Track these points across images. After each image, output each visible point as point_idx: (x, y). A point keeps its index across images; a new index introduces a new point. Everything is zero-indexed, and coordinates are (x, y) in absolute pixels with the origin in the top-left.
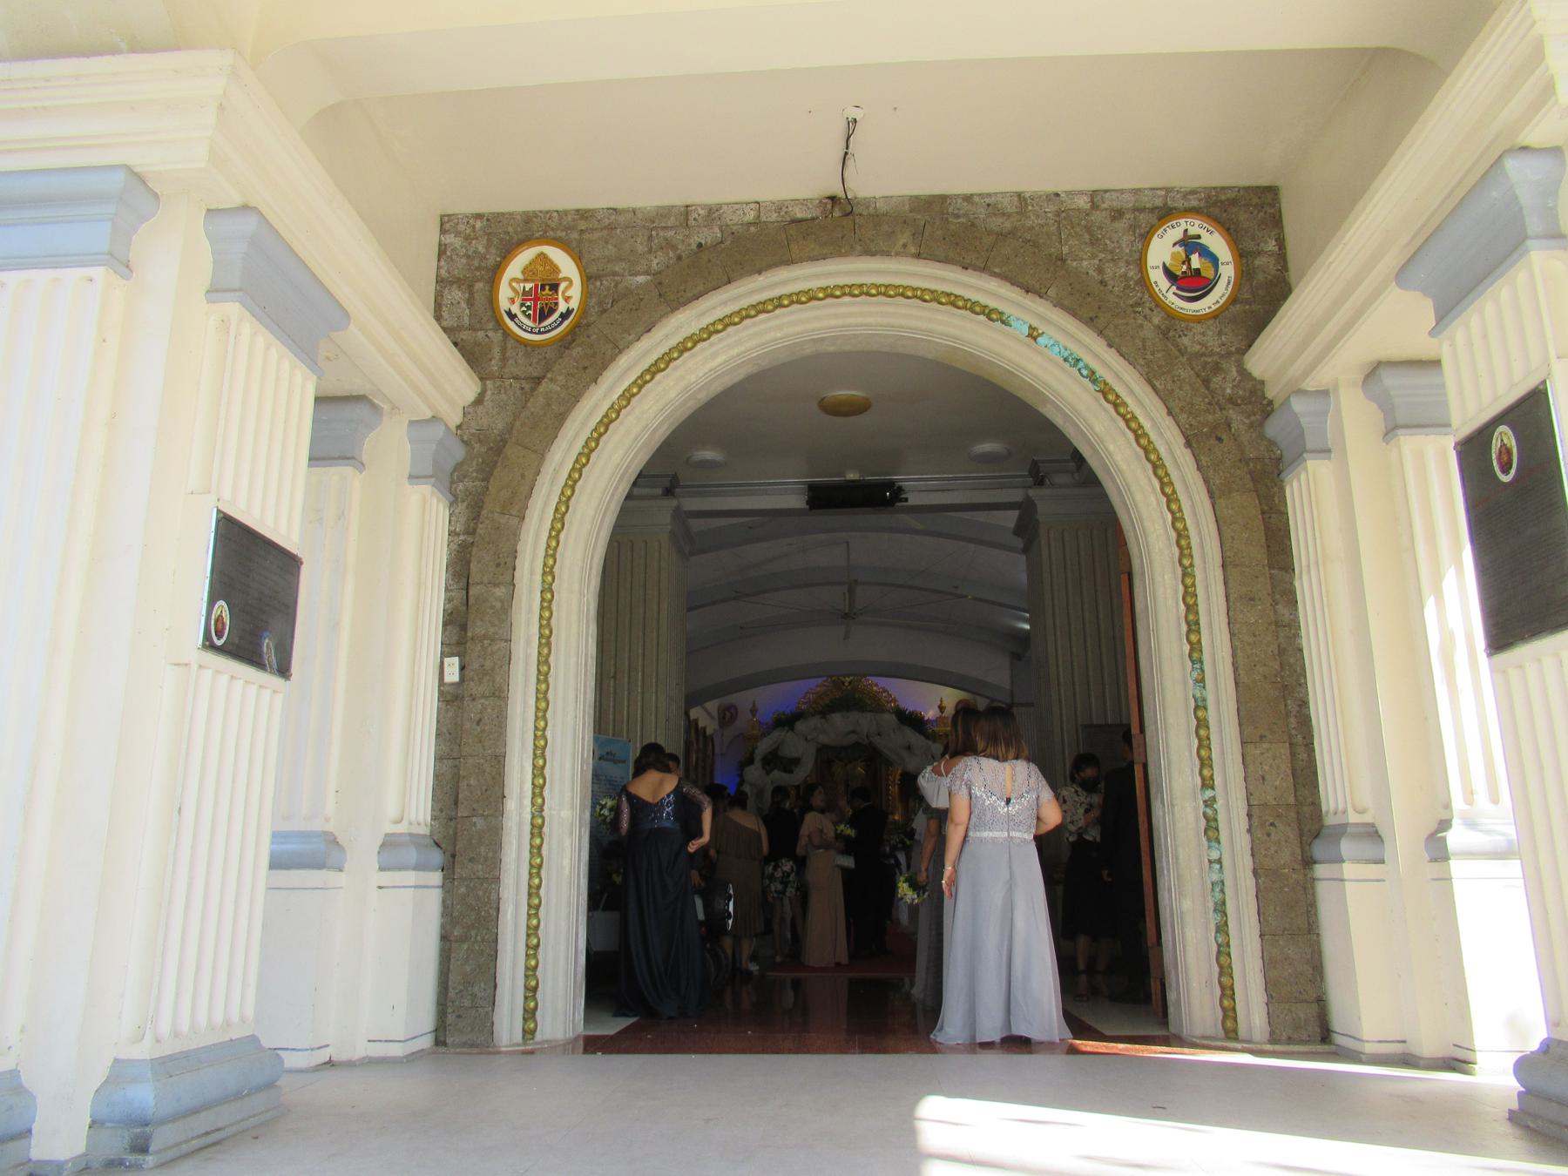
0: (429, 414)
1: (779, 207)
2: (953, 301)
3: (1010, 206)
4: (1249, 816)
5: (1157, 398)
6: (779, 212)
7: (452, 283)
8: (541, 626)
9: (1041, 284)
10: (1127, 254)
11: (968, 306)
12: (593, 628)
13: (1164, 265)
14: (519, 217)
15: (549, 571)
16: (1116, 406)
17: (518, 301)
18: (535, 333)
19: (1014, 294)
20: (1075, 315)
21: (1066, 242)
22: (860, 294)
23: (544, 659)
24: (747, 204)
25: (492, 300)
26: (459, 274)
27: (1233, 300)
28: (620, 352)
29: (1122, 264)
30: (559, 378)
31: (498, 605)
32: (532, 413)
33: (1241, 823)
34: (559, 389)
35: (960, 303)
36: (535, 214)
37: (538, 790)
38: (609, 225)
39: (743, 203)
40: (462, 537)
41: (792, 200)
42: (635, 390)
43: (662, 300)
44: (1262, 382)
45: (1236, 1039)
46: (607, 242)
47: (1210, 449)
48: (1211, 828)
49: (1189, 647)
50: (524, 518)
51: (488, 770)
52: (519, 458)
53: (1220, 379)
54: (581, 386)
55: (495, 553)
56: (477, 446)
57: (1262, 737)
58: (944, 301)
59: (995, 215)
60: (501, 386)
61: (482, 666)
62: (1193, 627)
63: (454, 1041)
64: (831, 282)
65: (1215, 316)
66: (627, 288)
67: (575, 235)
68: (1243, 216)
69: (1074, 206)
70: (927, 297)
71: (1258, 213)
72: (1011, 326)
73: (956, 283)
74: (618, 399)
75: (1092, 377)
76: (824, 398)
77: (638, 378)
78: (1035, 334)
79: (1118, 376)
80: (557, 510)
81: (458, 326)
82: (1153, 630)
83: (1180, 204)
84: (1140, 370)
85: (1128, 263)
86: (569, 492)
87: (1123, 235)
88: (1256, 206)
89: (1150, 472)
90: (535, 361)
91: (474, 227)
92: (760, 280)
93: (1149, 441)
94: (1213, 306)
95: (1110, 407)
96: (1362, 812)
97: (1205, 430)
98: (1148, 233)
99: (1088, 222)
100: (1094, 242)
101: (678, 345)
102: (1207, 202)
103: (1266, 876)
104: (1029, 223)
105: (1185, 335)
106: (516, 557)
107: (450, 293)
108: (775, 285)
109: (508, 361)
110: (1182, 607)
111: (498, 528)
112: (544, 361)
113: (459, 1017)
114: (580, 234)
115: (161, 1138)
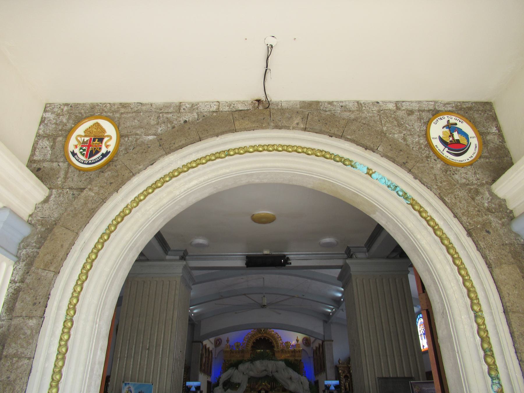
2: (324, 155)
5: (446, 207)
6: (230, 107)
7: (44, 137)
8: (60, 345)
9: (374, 145)
10: (418, 132)
11: (332, 157)
12: (104, 343)
13: (440, 137)
14: (88, 105)
15: (72, 308)
16: (420, 212)
17: (79, 147)
18: (86, 164)
19: (359, 150)
20: (394, 161)
21: (385, 125)
22: (273, 150)
23: (57, 370)
25: (65, 146)
26: (49, 132)
27: (480, 156)
28: (134, 175)
30: (95, 188)
31: (29, 332)
32: (75, 208)
35: (328, 156)
40: (18, 285)
42: (142, 198)
44: (504, 200)
46: (134, 119)
47: (484, 238)
49: (487, 366)
50: (59, 273)
52: (61, 234)
53: (480, 197)
54: (107, 193)
55: (34, 296)
56: (39, 227)
58: (319, 154)
59: (345, 111)
60: (61, 193)
61: (8, 378)
64: (257, 143)
65: (471, 164)
66: (142, 142)
68: (476, 116)
69: (387, 108)
70: (310, 152)
71: (484, 114)
72: (356, 168)
73: (327, 144)
74: (131, 202)
75: (405, 196)
76: (253, 215)
77: (144, 191)
78: (371, 172)
80: (84, 267)
81: (43, 159)
82: (458, 352)
83: (442, 108)
84: (435, 191)
85: (419, 136)
86: (93, 257)
88: (482, 111)
89: (445, 251)
91: (63, 110)
93: (442, 233)
94: (469, 159)
95: (417, 213)
97: (478, 226)
98: (428, 122)
99: (395, 116)
100: (400, 125)
101: (169, 173)
102: (456, 108)
104: (364, 115)
105: (456, 174)
106: (49, 298)
109: (68, 179)
110: (478, 338)
111: (39, 279)
112: (90, 179)
114: (121, 115)
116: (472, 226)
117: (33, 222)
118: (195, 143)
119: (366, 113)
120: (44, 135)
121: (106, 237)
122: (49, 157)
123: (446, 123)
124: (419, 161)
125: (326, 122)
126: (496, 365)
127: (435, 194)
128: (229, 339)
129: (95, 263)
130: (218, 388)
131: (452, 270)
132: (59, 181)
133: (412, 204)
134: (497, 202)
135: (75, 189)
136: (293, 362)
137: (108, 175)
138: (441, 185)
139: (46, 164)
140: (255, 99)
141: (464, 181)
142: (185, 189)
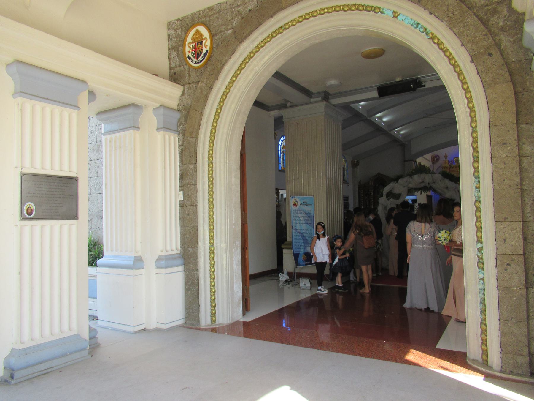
0: (158, 105)
7: (172, 49)
14: (190, 16)
28: (224, 65)
30: (204, 81)
31: (191, 172)
32: (197, 96)
33: (493, 262)
36: (195, 14)
37: (211, 238)
42: (234, 79)
43: (236, 39)
46: (218, 19)
48: (480, 262)
49: (474, 170)
50: (198, 138)
55: (189, 153)
57: (505, 219)
60: (189, 87)
61: (188, 194)
77: (234, 73)
79: (436, 29)
89: (457, 77)
90: (198, 74)
92: (273, 20)
103: (502, 290)
106: (197, 153)
107: (172, 53)
108: (279, 21)
109: (191, 76)
113: (189, 315)
114: (210, 18)
115: (17, 375)
116: (475, 52)
117: (180, 109)
118: (258, 28)
120: (172, 48)
121: (219, 111)
122: (178, 64)
128: (447, 155)
129: (217, 128)
130: (382, 198)
138: (452, 15)
139: (178, 69)
142: (262, 64)
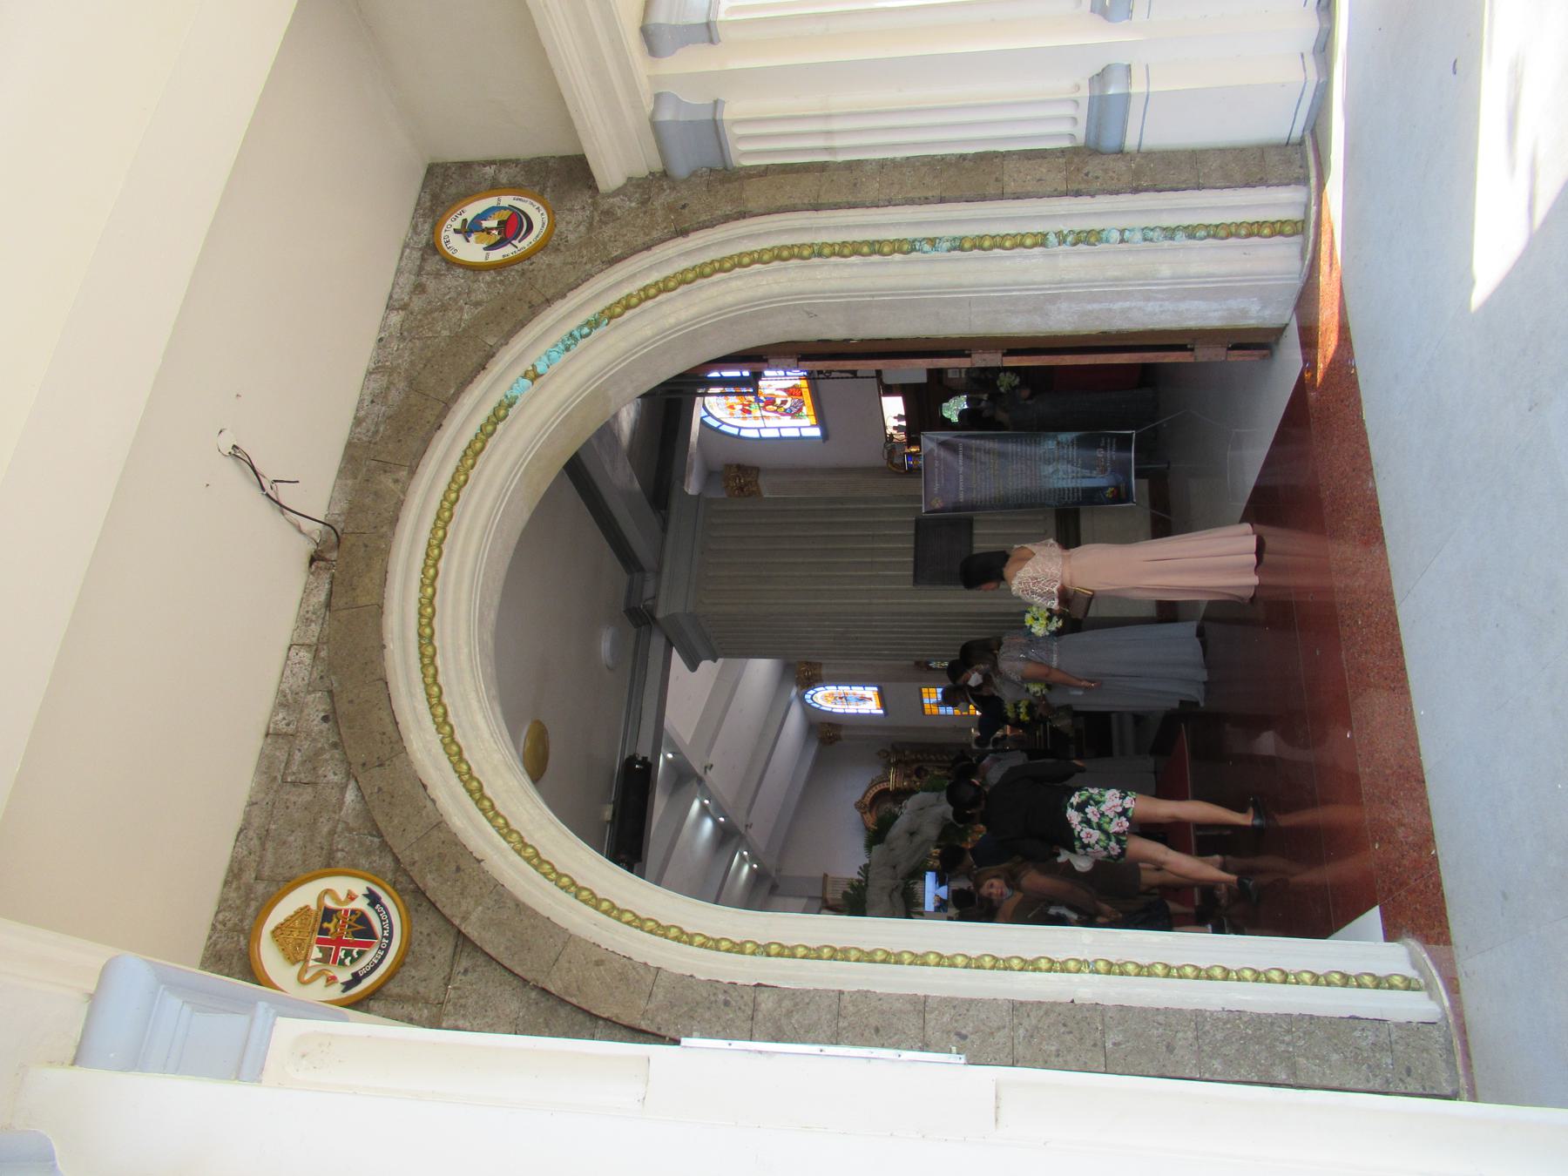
1: (304, 620)
2: (474, 452)
3: (379, 382)
4: (1078, 194)
6: (312, 621)
9: (480, 350)
13: (485, 249)
16: (628, 307)
17: (334, 970)
18: (389, 945)
19: (483, 382)
24: (288, 658)
27: (539, 197)
29: (475, 286)
30: (464, 908)
34: (480, 908)
35: (479, 445)
38: (260, 838)
39: (286, 665)
41: (300, 606)
42: (501, 821)
43: (387, 763)
44: (630, 179)
45: (1304, 222)
47: (694, 213)
51: (1034, 1022)
53: (619, 211)
60: (455, 1004)
62: (876, 248)
63: (1446, 1081)
64: (416, 576)
65: (552, 213)
66: (357, 816)
67: (260, 888)
68: (453, 190)
69: (399, 325)
71: (452, 178)
72: (517, 398)
73: (454, 441)
75: (593, 324)
78: (531, 374)
82: (873, 296)
87: (443, 284)
89: (705, 281)
90: (429, 951)
96: (1078, 88)
99: (420, 313)
100: (444, 308)
104: (406, 365)
105: (567, 237)
108: (403, 638)
109: (418, 993)
110: (853, 259)
112: (433, 935)
114: (262, 880)
118: (389, 694)
119: (400, 361)
123: (460, 237)
124: (530, 283)
125: (406, 428)
126: (895, 240)
127: (602, 270)
131: (739, 277)
132: (421, 1016)
133: (610, 318)
134: (631, 189)
135: (452, 970)
136: (876, 828)
137: (434, 879)
140: (308, 565)
141: (582, 229)
142: (492, 740)
